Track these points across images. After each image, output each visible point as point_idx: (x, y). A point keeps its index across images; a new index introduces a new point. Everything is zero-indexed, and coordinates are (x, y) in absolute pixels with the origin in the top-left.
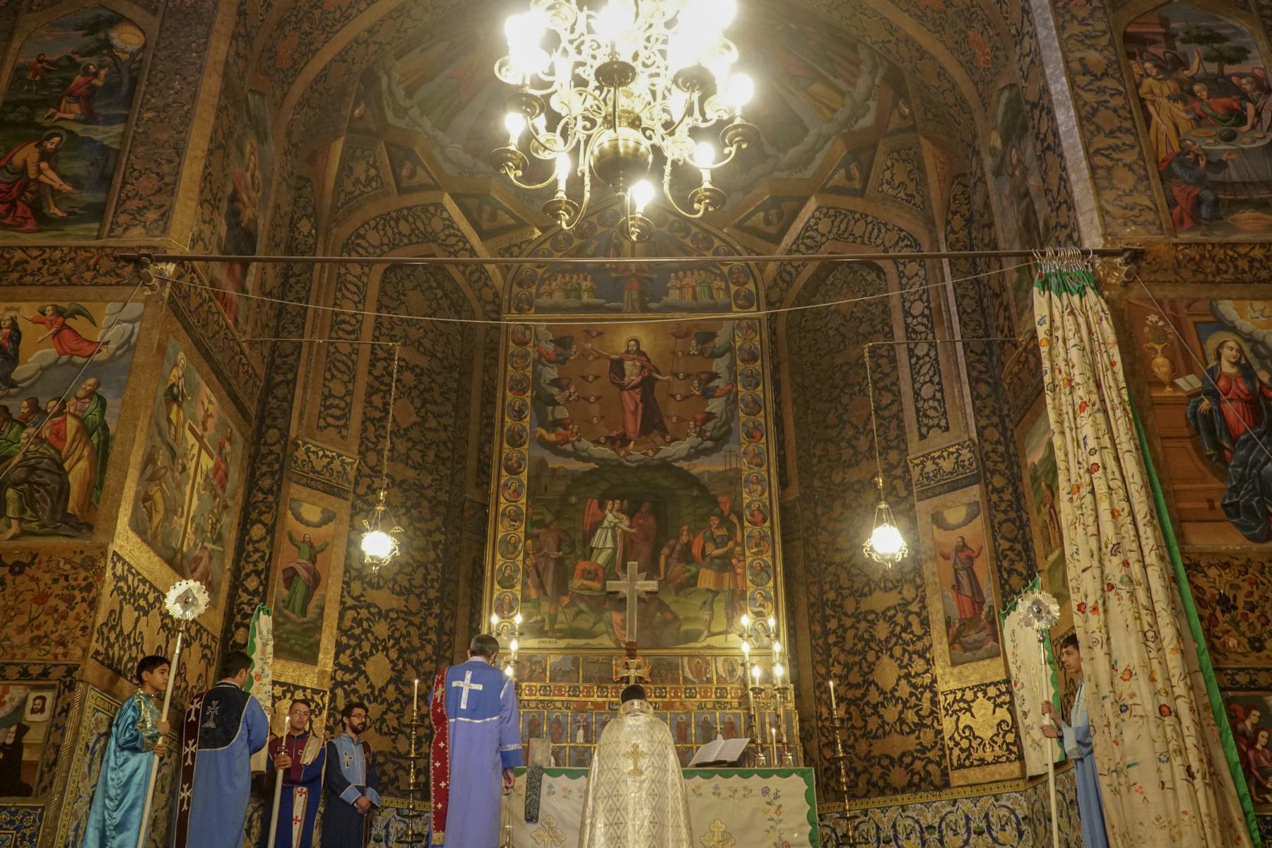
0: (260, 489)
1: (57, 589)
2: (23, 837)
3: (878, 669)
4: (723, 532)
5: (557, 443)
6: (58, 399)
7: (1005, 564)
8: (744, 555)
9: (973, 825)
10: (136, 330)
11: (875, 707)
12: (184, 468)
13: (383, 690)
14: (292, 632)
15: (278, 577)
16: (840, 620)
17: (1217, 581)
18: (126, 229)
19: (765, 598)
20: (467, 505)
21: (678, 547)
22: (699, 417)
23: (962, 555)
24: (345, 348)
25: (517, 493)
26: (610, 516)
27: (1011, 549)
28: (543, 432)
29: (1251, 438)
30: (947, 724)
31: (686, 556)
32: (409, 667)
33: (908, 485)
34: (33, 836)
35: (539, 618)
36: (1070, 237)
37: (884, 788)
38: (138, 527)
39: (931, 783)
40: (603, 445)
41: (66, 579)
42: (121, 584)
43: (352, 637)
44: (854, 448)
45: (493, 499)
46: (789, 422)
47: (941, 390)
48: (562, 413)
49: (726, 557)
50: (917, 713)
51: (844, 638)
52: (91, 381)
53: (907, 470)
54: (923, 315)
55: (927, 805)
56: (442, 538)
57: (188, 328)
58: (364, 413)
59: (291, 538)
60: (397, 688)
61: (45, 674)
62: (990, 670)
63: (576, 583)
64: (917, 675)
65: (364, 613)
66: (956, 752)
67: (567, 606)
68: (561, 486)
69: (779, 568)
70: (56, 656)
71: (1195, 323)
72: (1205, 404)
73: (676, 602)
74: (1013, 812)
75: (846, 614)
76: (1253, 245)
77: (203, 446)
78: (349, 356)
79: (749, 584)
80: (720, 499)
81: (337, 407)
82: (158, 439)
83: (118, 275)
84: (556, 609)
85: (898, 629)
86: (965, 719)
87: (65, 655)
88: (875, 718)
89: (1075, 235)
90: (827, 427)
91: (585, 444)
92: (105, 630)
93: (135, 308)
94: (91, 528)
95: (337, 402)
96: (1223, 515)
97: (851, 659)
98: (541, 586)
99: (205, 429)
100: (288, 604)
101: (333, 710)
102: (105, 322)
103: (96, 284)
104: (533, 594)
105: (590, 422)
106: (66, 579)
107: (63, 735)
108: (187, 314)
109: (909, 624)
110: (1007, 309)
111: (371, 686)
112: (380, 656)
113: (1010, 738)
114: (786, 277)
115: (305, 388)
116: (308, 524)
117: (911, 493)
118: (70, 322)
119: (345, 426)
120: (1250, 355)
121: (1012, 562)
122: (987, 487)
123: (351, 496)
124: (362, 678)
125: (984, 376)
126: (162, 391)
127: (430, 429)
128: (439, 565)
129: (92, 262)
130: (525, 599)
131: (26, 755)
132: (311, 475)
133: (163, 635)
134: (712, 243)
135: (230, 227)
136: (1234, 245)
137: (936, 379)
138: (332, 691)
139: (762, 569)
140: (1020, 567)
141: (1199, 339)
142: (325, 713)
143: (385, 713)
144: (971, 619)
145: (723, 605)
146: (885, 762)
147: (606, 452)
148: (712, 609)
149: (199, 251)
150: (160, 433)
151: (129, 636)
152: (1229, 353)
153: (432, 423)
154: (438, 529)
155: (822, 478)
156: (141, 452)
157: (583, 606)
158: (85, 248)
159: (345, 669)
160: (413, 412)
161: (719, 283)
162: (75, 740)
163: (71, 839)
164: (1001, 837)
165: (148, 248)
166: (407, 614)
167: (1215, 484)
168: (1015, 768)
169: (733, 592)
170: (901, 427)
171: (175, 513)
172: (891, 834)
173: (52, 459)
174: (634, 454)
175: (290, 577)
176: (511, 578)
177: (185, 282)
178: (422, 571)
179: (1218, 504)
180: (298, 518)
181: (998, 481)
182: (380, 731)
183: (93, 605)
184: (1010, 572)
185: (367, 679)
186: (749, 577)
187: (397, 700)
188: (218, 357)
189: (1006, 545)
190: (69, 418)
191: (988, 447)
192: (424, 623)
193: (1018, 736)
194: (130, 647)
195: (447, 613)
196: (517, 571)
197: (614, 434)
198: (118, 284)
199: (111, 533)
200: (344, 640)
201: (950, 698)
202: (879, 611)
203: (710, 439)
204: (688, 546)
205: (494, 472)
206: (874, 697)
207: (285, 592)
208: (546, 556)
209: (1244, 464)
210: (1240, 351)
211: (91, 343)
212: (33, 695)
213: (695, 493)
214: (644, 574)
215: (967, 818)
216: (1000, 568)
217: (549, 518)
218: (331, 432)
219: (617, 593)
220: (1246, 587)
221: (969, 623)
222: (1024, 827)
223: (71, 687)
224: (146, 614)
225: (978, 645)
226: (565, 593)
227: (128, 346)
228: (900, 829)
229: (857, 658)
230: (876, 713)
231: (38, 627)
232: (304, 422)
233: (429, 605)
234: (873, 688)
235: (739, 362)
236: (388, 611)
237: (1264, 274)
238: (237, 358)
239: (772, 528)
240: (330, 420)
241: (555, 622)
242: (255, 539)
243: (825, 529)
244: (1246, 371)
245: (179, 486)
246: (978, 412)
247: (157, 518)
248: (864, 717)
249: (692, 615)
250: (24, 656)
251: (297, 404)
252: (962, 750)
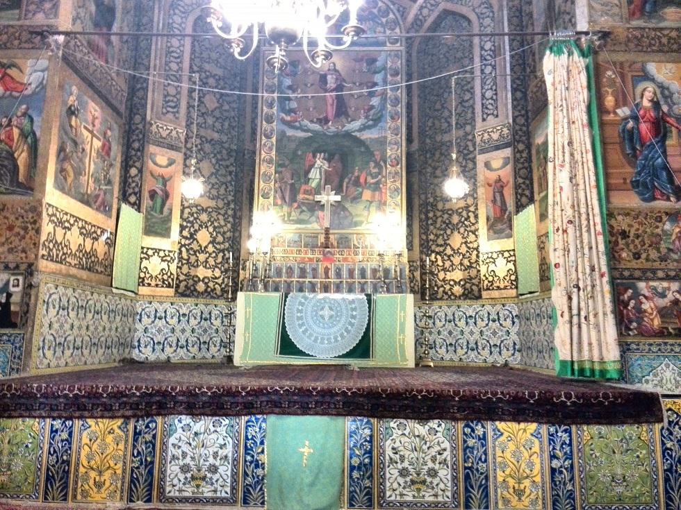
0: (133, 149)
1: (18, 223)
2: (16, 347)
3: (451, 238)
4: (376, 170)
5: (291, 122)
6: (7, 117)
7: (520, 191)
8: (386, 182)
9: (491, 317)
10: (46, 76)
11: (449, 256)
12: (83, 150)
13: (206, 247)
14: (157, 223)
15: (146, 195)
17: (622, 223)
18: (34, 14)
20: (246, 152)
21: (353, 178)
22: (366, 107)
23: (498, 185)
24: (174, 66)
25: (271, 149)
26: (318, 162)
27: (524, 183)
28: (284, 115)
29: (652, 144)
30: (483, 269)
31: (357, 183)
32: (219, 235)
33: (474, 145)
34: (20, 347)
36: (570, 20)
38: (61, 187)
39: (473, 295)
40: (315, 123)
41: (23, 217)
42: (53, 218)
43: (189, 222)
44: (448, 122)
45: (258, 153)
46: (415, 107)
47: (496, 94)
48: (294, 105)
49: (378, 183)
50: (469, 261)
52: (24, 107)
53: (474, 137)
54: (490, 50)
55: (470, 306)
56: (234, 169)
57: (76, 71)
58: (188, 103)
59: (152, 175)
60: (214, 246)
61: (17, 267)
62: (506, 244)
63: (300, 197)
64: (471, 242)
65: (194, 210)
66: (486, 282)
67: (297, 208)
68: (293, 146)
70: (21, 258)
71: (633, 76)
72: (631, 124)
74: (511, 312)
75: (438, 210)
76: (672, 29)
77: (93, 135)
78: (177, 71)
80: (375, 153)
81: (172, 101)
82: (64, 137)
83: (33, 43)
85: (463, 219)
86: (492, 267)
87: (26, 258)
89: (573, 20)
90: (435, 110)
91: (306, 122)
92: (46, 243)
93: (43, 63)
94: (32, 190)
95: (171, 98)
96: (630, 187)
97: (439, 232)
98: (283, 198)
99: (94, 126)
100: (153, 208)
101: (181, 259)
102: (28, 71)
103: (21, 48)
104: (279, 202)
105: (308, 110)
106: (23, 217)
107: (30, 298)
108: (75, 64)
109: (469, 217)
110: (534, 55)
111: (200, 246)
112: (204, 230)
113: (513, 278)
114: (419, 23)
115: (153, 91)
116: (161, 166)
117: (475, 149)
118: (9, 71)
119: (178, 112)
120: (659, 96)
121: (523, 190)
122: (514, 149)
123: (183, 150)
124: (195, 242)
125: (520, 87)
126: (65, 109)
127: (225, 111)
128: (233, 183)
129: (17, 34)
130: (275, 204)
131: (12, 308)
132: (161, 140)
133: (81, 238)
134: (377, 4)
135: (97, 6)
136: (662, 29)
137: (494, 88)
138: (180, 249)
139: (395, 190)
140: (527, 193)
141: (633, 86)
142: (176, 261)
143: (207, 258)
144: (499, 218)
146: (452, 283)
147: (317, 127)
148: (369, 211)
149: (78, 28)
150: (66, 133)
151: (61, 243)
152: (648, 95)
153: (226, 107)
154: (232, 164)
155: (430, 138)
156: (56, 147)
157: (304, 208)
158: (12, 26)
159: (186, 238)
160: (215, 101)
161: (380, 29)
162: (37, 300)
163: (41, 345)
164: (504, 323)
165: (48, 26)
166: (217, 209)
167: (629, 170)
168: (513, 292)
169: (380, 201)
170: (473, 113)
171: (80, 174)
172: (452, 318)
173: (7, 152)
174: (332, 128)
175: (153, 195)
177: (72, 43)
178: (224, 186)
179: (628, 181)
180: (155, 164)
181: (521, 147)
182: (205, 267)
183: (38, 231)
184: (522, 195)
186: (388, 194)
187: (214, 252)
188: (97, 84)
189: (521, 181)
190: (14, 128)
191: (517, 128)
192: (226, 213)
193: (517, 277)
194: (62, 248)
197: (321, 117)
198: (32, 48)
199: (43, 192)
200: (185, 224)
201: (486, 256)
203: (372, 120)
204: (358, 177)
205: (258, 137)
206: (449, 251)
207: (151, 203)
209: (646, 159)
210: (655, 94)
211: (22, 84)
212: (12, 278)
213: (363, 149)
214: (334, 192)
215: (489, 314)
216: (516, 193)
217: (287, 163)
218: (170, 116)
219: (320, 202)
220: (636, 226)
221: (499, 219)
222: (515, 320)
223: (31, 274)
224: (69, 229)
225: (501, 231)
226: (296, 201)
227: (42, 86)
228: (456, 316)
229: (442, 232)
231: (11, 243)
232: (155, 110)
233: (228, 204)
234: (448, 247)
235: (389, 76)
237: (675, 47)
238: (110, 83)
239: (401, 168)
240: (169, 109)
242: (132, 175)
243: (430, 165)
244: (656, 105)
245: (81, 160)
246: (514, 107)
247: (70, 180)
248: (443, 261)
249: (359, 213)
250: (5, 258)
251: (149, 102)
252: (489, 282)
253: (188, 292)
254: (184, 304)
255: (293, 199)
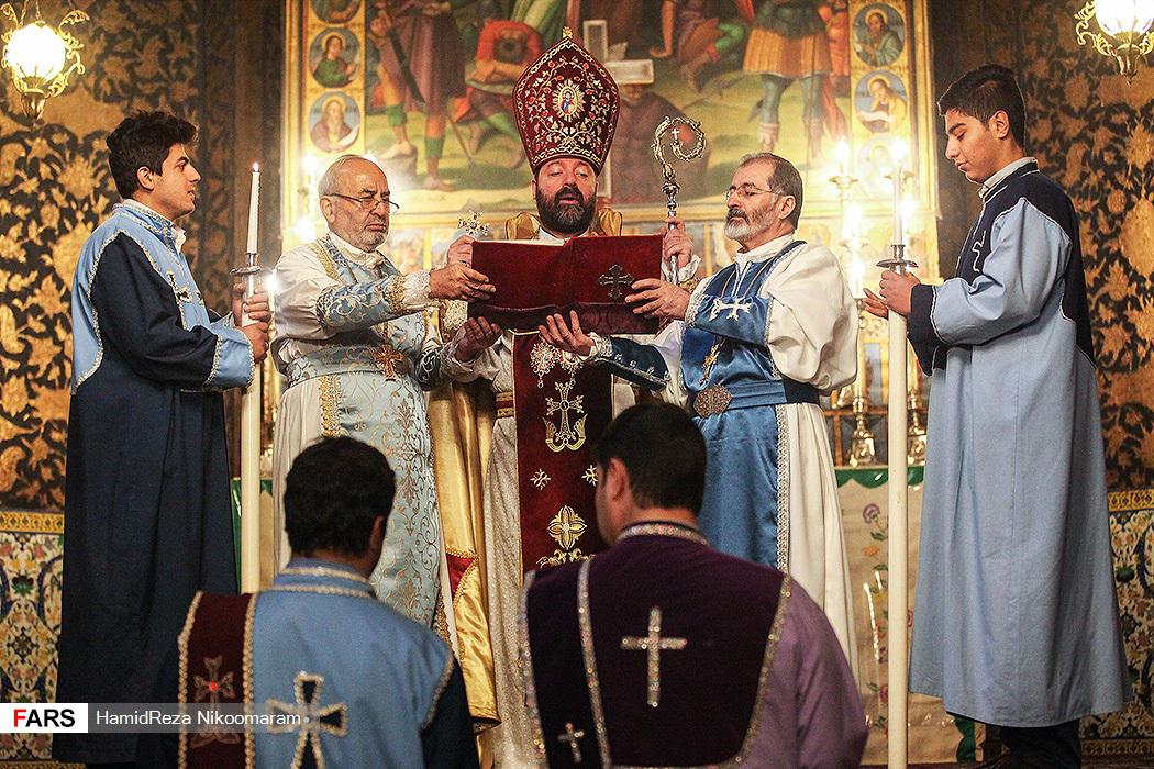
11: (1120, 307)
16: (1055, 123)
19: (890, 92)
35: (405, 147)
37: (1130, 470)
43: (20, 199)
51: (1063, 163)
63: (480, 71)
65: (39, 147)
69: (921, 26)
73: (696, 104)
75: (1069, 111)
79: (856, 60)
84: (441, 127)
88: (1118, 329)
98: (406, 81)
104: (390, 97)
124: (48, 282)
128: (193, 29)
130: (373, 108)
139: (885, 28)
145: (800, 108)
157: (498, 119)
169: (823, 78)
176: (341, 63)
178: (156, 43)
185: (59, 283)
195: (214, 131)
196: (356, 46)
202: (1136, 106)
208: (415, 12)
226: (459, 90)
230: (1121, 318)
234: (1116, 268)
236: (89, 138)
241: (439, 157)
249: (731, 132)
253: (31, 491)
254: (23, 537)
255: (450, 82)
